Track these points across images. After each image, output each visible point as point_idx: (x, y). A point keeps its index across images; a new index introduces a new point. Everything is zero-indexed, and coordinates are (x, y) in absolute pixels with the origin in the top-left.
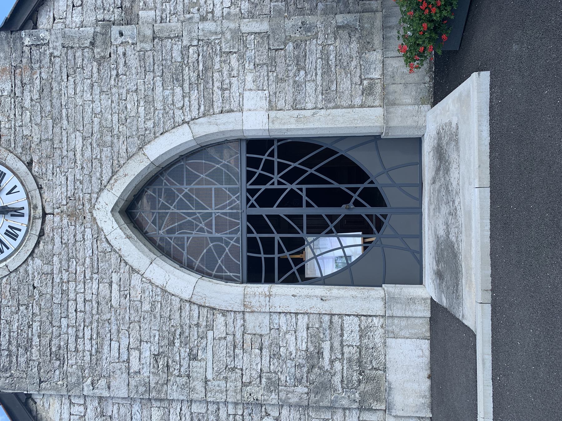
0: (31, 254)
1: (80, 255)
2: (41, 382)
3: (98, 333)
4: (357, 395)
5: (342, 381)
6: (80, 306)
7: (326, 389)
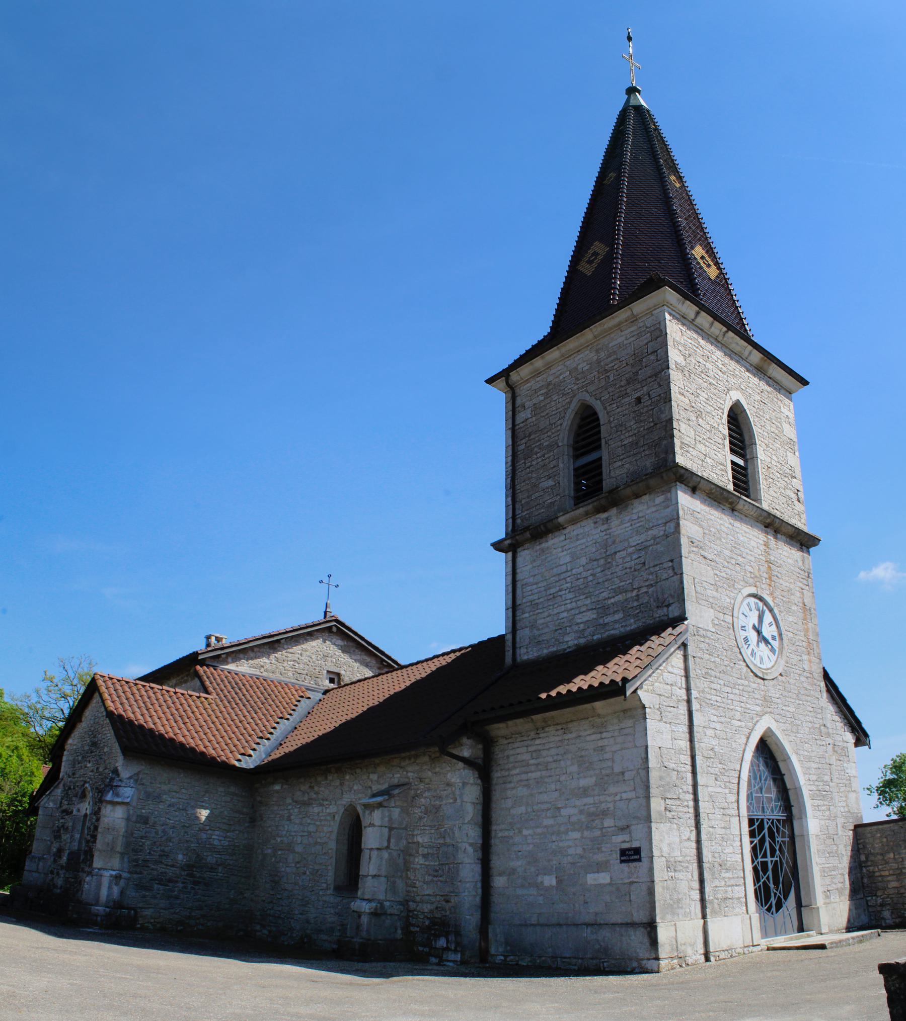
0: (747, 666)
1: (749, 701)
2: (694, 657)
3: (719, 707)
4: (712, 898)
5: (716, 887)
6: (731, 696)
7: (712, 875)
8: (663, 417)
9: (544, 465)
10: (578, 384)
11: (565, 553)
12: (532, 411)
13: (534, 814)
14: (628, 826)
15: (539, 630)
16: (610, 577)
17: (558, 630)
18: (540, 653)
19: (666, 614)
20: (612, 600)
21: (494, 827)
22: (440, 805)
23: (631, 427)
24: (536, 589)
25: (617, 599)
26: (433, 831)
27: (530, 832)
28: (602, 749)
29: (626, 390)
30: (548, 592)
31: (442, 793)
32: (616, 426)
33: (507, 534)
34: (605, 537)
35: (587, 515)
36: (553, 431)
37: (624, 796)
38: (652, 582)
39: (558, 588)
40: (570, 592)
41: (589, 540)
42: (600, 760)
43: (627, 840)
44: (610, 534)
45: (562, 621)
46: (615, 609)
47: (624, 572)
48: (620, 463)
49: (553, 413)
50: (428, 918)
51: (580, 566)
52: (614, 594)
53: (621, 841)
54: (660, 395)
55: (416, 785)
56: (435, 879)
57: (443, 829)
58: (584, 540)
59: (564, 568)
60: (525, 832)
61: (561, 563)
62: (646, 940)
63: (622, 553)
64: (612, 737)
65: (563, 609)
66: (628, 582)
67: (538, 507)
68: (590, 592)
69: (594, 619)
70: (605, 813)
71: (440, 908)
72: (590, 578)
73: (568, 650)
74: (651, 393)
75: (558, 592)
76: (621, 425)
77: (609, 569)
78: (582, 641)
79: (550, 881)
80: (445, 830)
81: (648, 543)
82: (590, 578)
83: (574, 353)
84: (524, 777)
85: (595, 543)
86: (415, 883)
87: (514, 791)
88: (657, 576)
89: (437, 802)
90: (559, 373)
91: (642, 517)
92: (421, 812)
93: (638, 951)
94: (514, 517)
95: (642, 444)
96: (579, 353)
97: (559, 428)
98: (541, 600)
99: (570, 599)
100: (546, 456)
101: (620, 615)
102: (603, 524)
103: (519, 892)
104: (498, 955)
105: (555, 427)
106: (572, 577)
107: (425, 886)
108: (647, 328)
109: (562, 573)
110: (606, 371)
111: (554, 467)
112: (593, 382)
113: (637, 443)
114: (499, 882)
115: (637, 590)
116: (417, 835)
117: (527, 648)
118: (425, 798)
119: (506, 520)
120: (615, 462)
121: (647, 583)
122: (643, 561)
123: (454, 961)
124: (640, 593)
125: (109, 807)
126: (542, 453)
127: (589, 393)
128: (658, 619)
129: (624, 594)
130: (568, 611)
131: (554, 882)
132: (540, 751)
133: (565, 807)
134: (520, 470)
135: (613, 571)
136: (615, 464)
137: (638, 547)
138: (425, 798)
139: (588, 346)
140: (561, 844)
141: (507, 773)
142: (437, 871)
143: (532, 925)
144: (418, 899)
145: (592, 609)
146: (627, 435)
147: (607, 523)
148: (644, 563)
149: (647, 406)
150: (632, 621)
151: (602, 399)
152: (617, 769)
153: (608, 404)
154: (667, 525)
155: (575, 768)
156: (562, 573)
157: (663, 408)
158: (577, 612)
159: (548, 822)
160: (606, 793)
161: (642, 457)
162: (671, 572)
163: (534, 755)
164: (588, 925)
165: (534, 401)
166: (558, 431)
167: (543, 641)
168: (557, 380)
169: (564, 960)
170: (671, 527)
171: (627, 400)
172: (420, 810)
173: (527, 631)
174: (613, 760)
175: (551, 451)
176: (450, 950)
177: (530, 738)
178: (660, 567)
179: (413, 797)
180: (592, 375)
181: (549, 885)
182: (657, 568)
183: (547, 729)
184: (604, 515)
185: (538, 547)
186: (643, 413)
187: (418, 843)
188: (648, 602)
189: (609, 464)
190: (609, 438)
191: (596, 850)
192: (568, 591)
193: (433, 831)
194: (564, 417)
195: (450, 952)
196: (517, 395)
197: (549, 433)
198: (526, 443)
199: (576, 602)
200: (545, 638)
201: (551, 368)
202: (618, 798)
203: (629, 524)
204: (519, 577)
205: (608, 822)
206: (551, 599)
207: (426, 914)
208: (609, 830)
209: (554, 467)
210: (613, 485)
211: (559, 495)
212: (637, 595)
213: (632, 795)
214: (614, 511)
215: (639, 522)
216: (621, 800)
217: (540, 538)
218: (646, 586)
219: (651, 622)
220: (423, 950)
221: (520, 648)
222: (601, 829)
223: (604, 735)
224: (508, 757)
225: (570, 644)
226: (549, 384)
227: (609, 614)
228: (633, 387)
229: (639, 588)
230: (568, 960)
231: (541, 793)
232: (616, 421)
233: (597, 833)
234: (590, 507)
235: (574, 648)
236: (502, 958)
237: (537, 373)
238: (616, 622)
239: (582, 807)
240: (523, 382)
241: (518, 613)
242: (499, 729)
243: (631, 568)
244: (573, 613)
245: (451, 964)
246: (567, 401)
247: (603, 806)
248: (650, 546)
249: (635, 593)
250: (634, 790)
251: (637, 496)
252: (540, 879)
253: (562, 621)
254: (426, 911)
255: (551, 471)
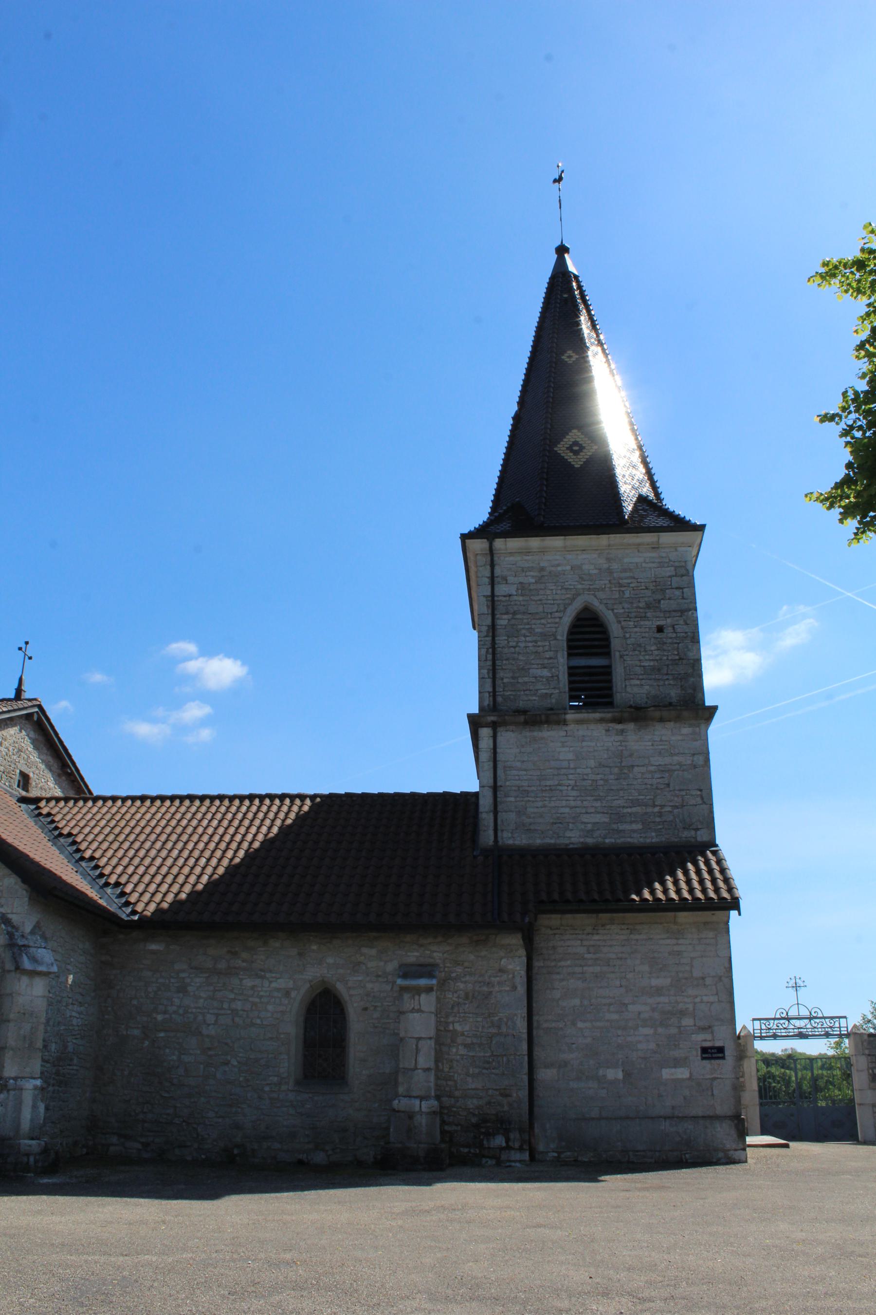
8: (691, 655)
9: (536, 652)
10: (583, 584)
11: (567, 749)
12: (518, 589)
13: (592, 1007)
14: (710, 1027)
15: (530, 818)
16: (626, 787)
17: (555, 823)
18: (531, 841)
19: (694, 836)
20: (629, 810)
21: (535, 1018)
22: (491, 993)
23: (652, 651)
24: (525, 775)
25: (634, 810)
26: (479, 1019)
27: (588, 1024)
28: (679, 953)
29: (646, 613)
30: (543, 783)
31: (493, 979)
32: (633, 644)
33: (481, 708)
34: (620, 748)
35: (602, 720)
36: (549, 621)
37: (705, 999)
38: (677, 804)
39: (556, 783)
40: (573, 789)
41: (598, 745)
42: (676, 964)
43: (708, 1039)
44: (626, 746)
45: (563, 815)
46: (633, 819)
47: (644, 786)
48: (638, 682)
49: (549, 602)
50: (474, 1115)
51: (587, 767)
52: (631, 805)
53: (702, 1039)
54: (686, 633)
55: (448, 967)
56: (485, 1071)
57: (497, 1018)
58: (593, 744)
59: (565, 764)
60: (580, 1025)
61: (561, 758)
62: (733, 1132)
63: (642, 768)
64: (690, 944)
65: (564, 805)
66: (648, 797)
67: (527, 692)
68: (599, 796)
69: (604, 822)
70: (683, 1013)
71: (494, 1103)
72: (601, 782)
73: (571, 846)
74: (675, 626)
75: (557, 785)
76: (640, 645)
77: (624, 779)
78: (590, 841)
79: (615, 1074)
80: (500, 1019)
81: (674, 768)
82: (601, 782)
83: (578, 550)
84: (578, 970)
85: (608, 750)
86: (453, 1076)
87: (564, 983)
88: (683, 800)
89: (485, 989)
90: (557, 562)
91: (666, 741)
92: (458, 997)
93: (725, 1142)
94: (494, 694)
95: (666, 672)
96: (584, 552)
97: (557, 620)
98: (533, 788)
99: (574, 796)
100: (539, 643)
101: (639, 826)
102: (617, 735)
103: (573, 1085)
104: (550, 1152)
105: (551, 618)
106: (576, 775)
107: (469, 1079)
108: (670, 561)
109: (562, 768)
110: (621, 586)
111: (551, 658)
112: (603, 590)
113: (659, 670)
114: (544, 1075)
115: (658, 808)
116: (453, 1023)
117: (512, 833)
118: (465, 982)
119: (480, 692)
120: (633, 679)
121: (671, 804)
122: (666, 782)
123: (520, 1161)
124: (663, 810)
125: (25, 980)
126: (534, 638)
127: (598, 599)
128: (684, 839)
129: (644, 808)
130: (571, 808)
131: (620, 1075)
132: (599, 946)
133: (633, 1003)
134: (501, 646)
135: (630, 783)
136: (632, 681)
137: (661, 768)
138: (465, 982)
139: (597, 550)
140: (629, 1039)
141: (553, 964)
142: (488, 1062)
143: (593, 1119)
144: (457, 1093)
145: (604, 813)
146: (647, 657)
147: (622, 735)
148: (668, 785)
149: (671, 638)
150: (653, 834)
151: (616, 611)
152: (697, 973)
153: (623, 619)
154: (696, 756)
155: (646, 968)
156: (562, 768)
157: (690, 647)
158: (584, 811)
159: (615, 1017)
160: (683, 994)
161: (664, 685)
162: (699, 800)
163: (592, 949)
164: (665, 1118)
165: (521, 579)
166: (556, 623)
167: (535, 830)
168: (553, 569)
169: (637, 1153)
170: (700, 760)
171: (647, 623)
172: (456, 995)
173: (512, 816)
174: (692, 966)
175: (545, 640)
176: (513, 1149)
177: (585, 932)
178: (686, 793)
179: (444, 981)
180: (602, 582)
181: (613, 1079)
182: (684, 793)
183: (608, 927)
184: (620, 727)
185: (528, 734)
186: (666, 643)
187: (455, 1031)
188: (672, 821)
189: (625, 680)
190: (625, 653)
191: (673, 1047)
192: (570, 788)
193: (479, 1019)
194: (564, 611)
195: (513, 1152)
196: (495, 563)
197: (543, 621)
198: (509, 620)
199: (582, 801)
200: (539, 828)
201: (545, 554)
202: (698, 1000)
203: (650, 743)
204: (500, 757)
205: (687, 1022)
206: (546, 790)
207: (471, 1110)
208: (688, 1028)
209: (551, 658)
210: (630, 701)
211: (559, 688)
212: (660, 812)
213: (712, 999)
214: (631, 726)
215: (661, 745)
216: (702, 1002)
217: (532, 725)
218: (670, 806)
219: (676, 840)
220: (469, 1152)
221: (502, 831)
222: (679, 1027)
223: (681, 941)
224: (554, 948)
225: (573, 840)
226: (542, 569)
227: (626, 822)
228: (654, 613)
229: (662, 806)
230: (642, 1153)
231: (601, 987)
232: (633, 640)
233: (673, 1031)
234: (609, 716)
235: (580, 846)
236: (555, 1154)
237: (528, 552)
238: (634, 831)
239: (655, 1006)
240: (505, 553)
241: (500, 794)
242: (548, 921)
243: (652, 785)
244: (578, 811)
245: (518, 1164)
246: (568, 596)
247: (681, 1006)
248: (675, 770)
249: (657, 809)
250: (717, 994)
251: (661, 720)
252: (601, 1072)
253: (563, 815)
254: (471, 1106)
255: (546, 661)
